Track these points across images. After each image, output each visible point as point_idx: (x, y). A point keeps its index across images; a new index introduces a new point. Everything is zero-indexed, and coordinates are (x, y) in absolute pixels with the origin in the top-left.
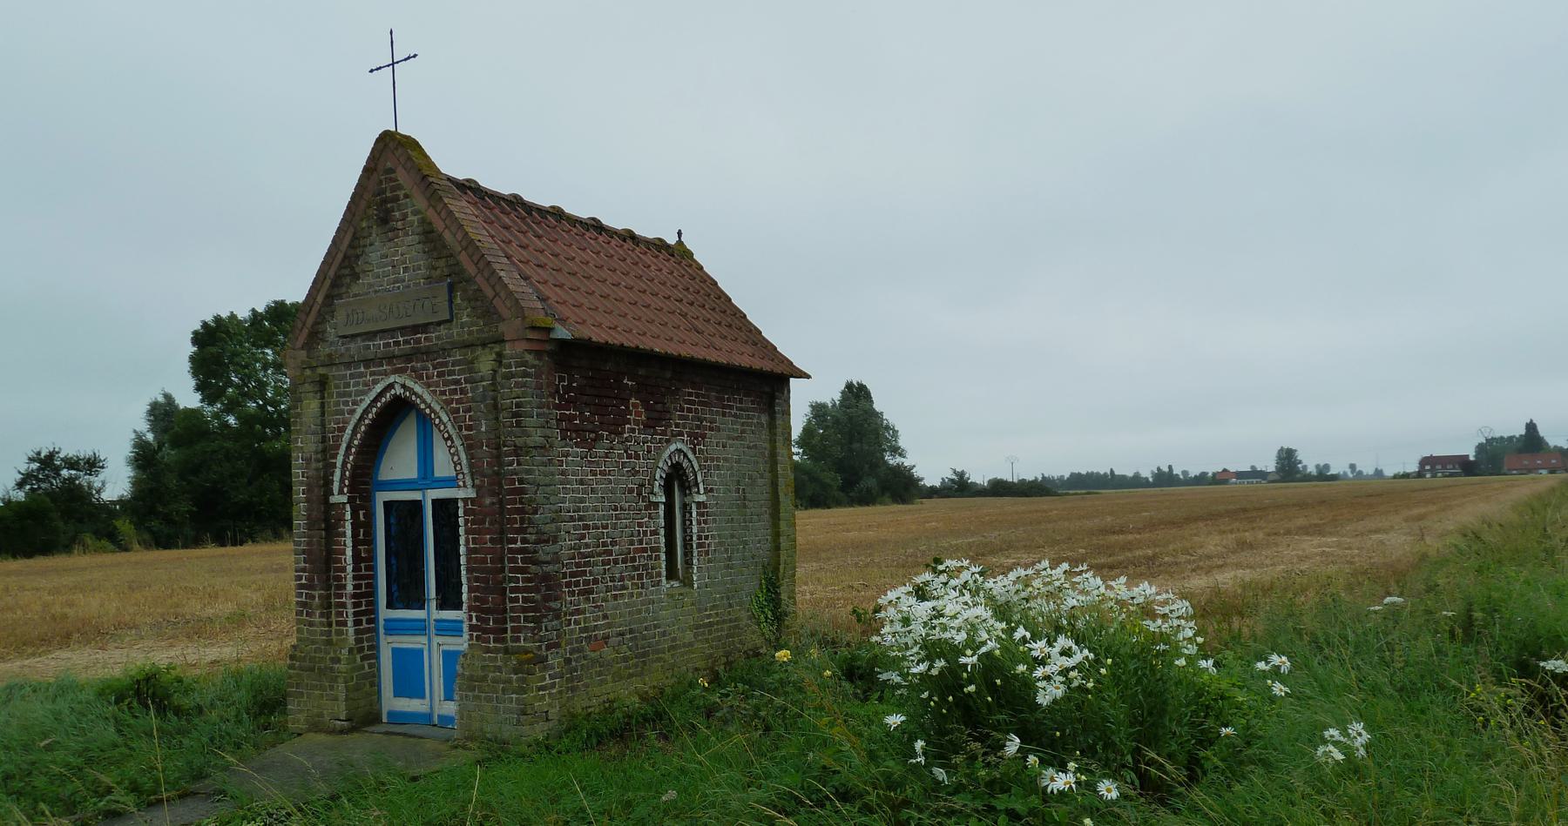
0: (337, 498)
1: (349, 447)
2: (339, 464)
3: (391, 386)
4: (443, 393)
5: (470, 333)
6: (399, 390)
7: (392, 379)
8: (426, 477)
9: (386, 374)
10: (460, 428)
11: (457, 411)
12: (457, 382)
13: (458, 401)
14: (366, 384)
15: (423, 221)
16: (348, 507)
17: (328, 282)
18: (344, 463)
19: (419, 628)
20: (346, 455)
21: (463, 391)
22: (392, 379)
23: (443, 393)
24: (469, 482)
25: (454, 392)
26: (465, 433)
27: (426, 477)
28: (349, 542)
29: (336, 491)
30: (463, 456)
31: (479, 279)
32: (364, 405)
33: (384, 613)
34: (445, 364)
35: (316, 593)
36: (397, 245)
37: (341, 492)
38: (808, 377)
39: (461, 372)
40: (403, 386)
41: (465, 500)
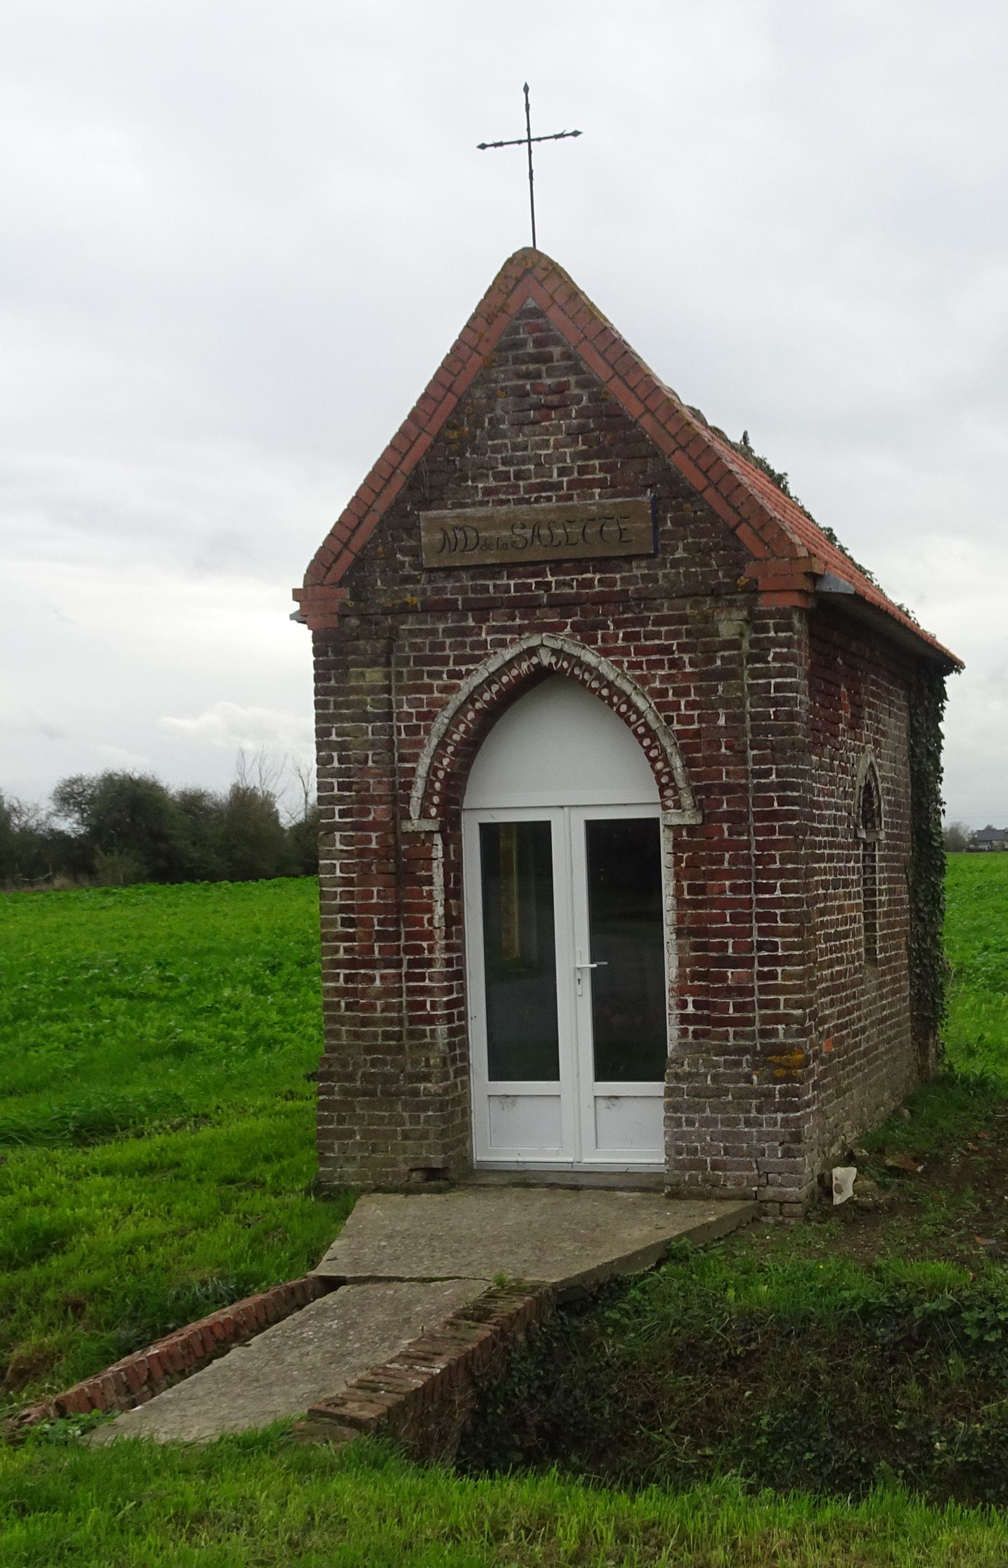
0: (415, 824)
1: (442, 745)
2: (422, 770)
3: (532, 652)
4: (638, 665)
5: (687, 575)
6: (546, 659)
7: (535, 641)
9: (520, 630)
10: (669, 720)
11: (663, 693)
12: (667, 650)
13: (664, 679)
14: (483, 645)
15: (594, 398)
16: (438, 839)
17: (398, 482)
18: (433, 770)
20: (437, 757)
21: (674, 664)
22: (535, 641)
23: (638, 665)
24: (687, 800)
26: (676, 727)
28: (439, 896)
29: (414, 808)
30: (677, 762)
31: (709, 495)
32: (476, 680)
34: (643, 622)
35: (377, 973)
36: (547, 431)
37: (424, 814)
39: (673, 635)
40: (555, 652)
41: (677, 829)
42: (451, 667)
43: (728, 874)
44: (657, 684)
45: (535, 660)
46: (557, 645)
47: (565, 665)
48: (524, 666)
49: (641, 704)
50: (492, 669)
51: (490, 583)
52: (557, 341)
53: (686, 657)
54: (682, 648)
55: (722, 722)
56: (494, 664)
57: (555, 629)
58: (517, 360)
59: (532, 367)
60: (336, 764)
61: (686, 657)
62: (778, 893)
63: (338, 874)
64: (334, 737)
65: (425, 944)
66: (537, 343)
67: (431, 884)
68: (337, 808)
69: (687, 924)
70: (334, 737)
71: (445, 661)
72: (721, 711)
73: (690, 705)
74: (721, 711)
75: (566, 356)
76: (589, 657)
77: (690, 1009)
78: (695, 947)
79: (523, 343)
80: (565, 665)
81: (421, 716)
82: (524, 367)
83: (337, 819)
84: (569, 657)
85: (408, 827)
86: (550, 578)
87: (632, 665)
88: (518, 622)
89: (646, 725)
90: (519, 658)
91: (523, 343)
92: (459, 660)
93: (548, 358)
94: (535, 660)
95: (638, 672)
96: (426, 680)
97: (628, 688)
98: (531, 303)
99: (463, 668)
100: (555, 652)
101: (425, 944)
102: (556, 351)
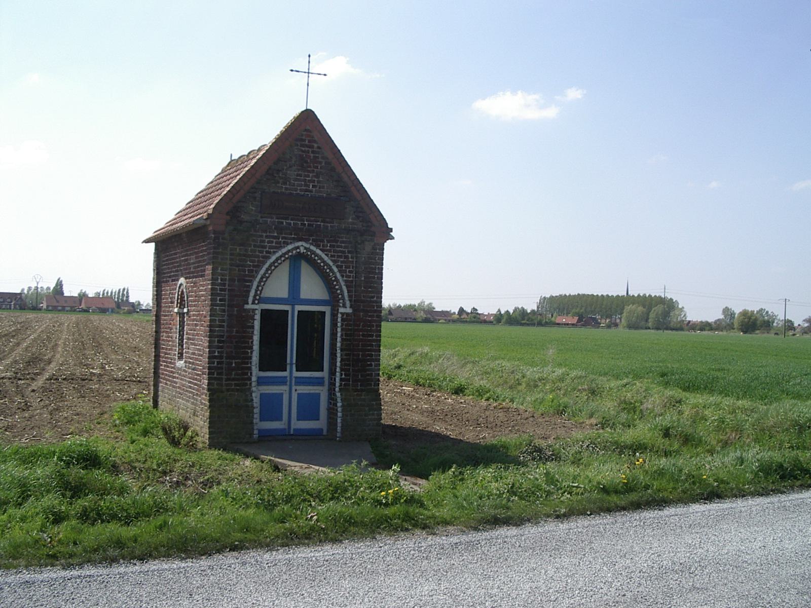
2: (254, 287)
3: (298, 248)
6: (302, 250)
8: (294, 296)
10: (342, 276)
12: (343, 252)
13: (342, 262)
19: (282, 381)
22: (300, 243)
25: (341, 257)
27: (294, 296)
29: (250, 299)
33: (255, 372)
37: (253, 303)
38: (143, 242)
39: (345, 247)
40: (305, 248)
42: (267, 249)
43: (361, 330)
44: (339, 264)
45: (298, 250)
46: (307, 246)
47: (309, 253)
48: (294, 252)
49: (336, 270)
50: (283, 252)
51: (284, 221)
52: (315, 142)
53: (350, 255)
54: (349, 252)
55: (363, 279)
56: (284, 250)
57: (306, 241)
58: (302, 146)
59: (307, 149)
60: (219, 281)
61: (350, 255)
62: (374, 338)
63: (217, 323)
64: (219, 271)
65: (249, 351)
66: (309, 141)
67: (253, 328)
68: (218, 298)
69: (344, 347)
70: (219, 271)
71: (265, 247)
72: (363, 275)
73: (350, 272)
74: (363, 275)
75: (319, 148)
76: (318, 252)
77: (343, 376)
78: (346, 355)
79: (304, 140)
80: (309, 253)
81: (254, 266)
82: (303, 149)
83: (218, 302)
84: (311, 251)
85: (246, 307)
86: (306, 222)
87: (332, 256)
88: (293, 236)
89: (336, 277)
90: (293, 249)
91: (304, 140)
92: (271, 247)
93: (313, 147)
94: (298, 250)
95: (333, 259)
96: (257, 253)
97: (331, 264)
98: (308, 127)
99: (272, 250)
100: (305, 248)
101: (249, 351)
102: (316, 145)
